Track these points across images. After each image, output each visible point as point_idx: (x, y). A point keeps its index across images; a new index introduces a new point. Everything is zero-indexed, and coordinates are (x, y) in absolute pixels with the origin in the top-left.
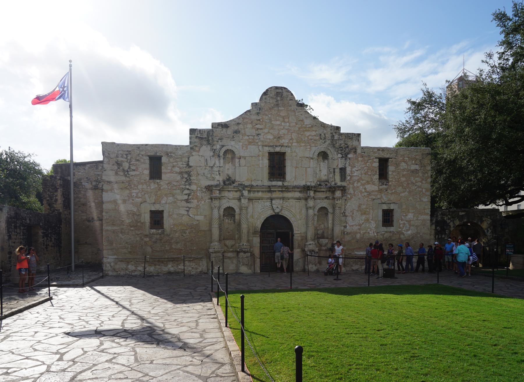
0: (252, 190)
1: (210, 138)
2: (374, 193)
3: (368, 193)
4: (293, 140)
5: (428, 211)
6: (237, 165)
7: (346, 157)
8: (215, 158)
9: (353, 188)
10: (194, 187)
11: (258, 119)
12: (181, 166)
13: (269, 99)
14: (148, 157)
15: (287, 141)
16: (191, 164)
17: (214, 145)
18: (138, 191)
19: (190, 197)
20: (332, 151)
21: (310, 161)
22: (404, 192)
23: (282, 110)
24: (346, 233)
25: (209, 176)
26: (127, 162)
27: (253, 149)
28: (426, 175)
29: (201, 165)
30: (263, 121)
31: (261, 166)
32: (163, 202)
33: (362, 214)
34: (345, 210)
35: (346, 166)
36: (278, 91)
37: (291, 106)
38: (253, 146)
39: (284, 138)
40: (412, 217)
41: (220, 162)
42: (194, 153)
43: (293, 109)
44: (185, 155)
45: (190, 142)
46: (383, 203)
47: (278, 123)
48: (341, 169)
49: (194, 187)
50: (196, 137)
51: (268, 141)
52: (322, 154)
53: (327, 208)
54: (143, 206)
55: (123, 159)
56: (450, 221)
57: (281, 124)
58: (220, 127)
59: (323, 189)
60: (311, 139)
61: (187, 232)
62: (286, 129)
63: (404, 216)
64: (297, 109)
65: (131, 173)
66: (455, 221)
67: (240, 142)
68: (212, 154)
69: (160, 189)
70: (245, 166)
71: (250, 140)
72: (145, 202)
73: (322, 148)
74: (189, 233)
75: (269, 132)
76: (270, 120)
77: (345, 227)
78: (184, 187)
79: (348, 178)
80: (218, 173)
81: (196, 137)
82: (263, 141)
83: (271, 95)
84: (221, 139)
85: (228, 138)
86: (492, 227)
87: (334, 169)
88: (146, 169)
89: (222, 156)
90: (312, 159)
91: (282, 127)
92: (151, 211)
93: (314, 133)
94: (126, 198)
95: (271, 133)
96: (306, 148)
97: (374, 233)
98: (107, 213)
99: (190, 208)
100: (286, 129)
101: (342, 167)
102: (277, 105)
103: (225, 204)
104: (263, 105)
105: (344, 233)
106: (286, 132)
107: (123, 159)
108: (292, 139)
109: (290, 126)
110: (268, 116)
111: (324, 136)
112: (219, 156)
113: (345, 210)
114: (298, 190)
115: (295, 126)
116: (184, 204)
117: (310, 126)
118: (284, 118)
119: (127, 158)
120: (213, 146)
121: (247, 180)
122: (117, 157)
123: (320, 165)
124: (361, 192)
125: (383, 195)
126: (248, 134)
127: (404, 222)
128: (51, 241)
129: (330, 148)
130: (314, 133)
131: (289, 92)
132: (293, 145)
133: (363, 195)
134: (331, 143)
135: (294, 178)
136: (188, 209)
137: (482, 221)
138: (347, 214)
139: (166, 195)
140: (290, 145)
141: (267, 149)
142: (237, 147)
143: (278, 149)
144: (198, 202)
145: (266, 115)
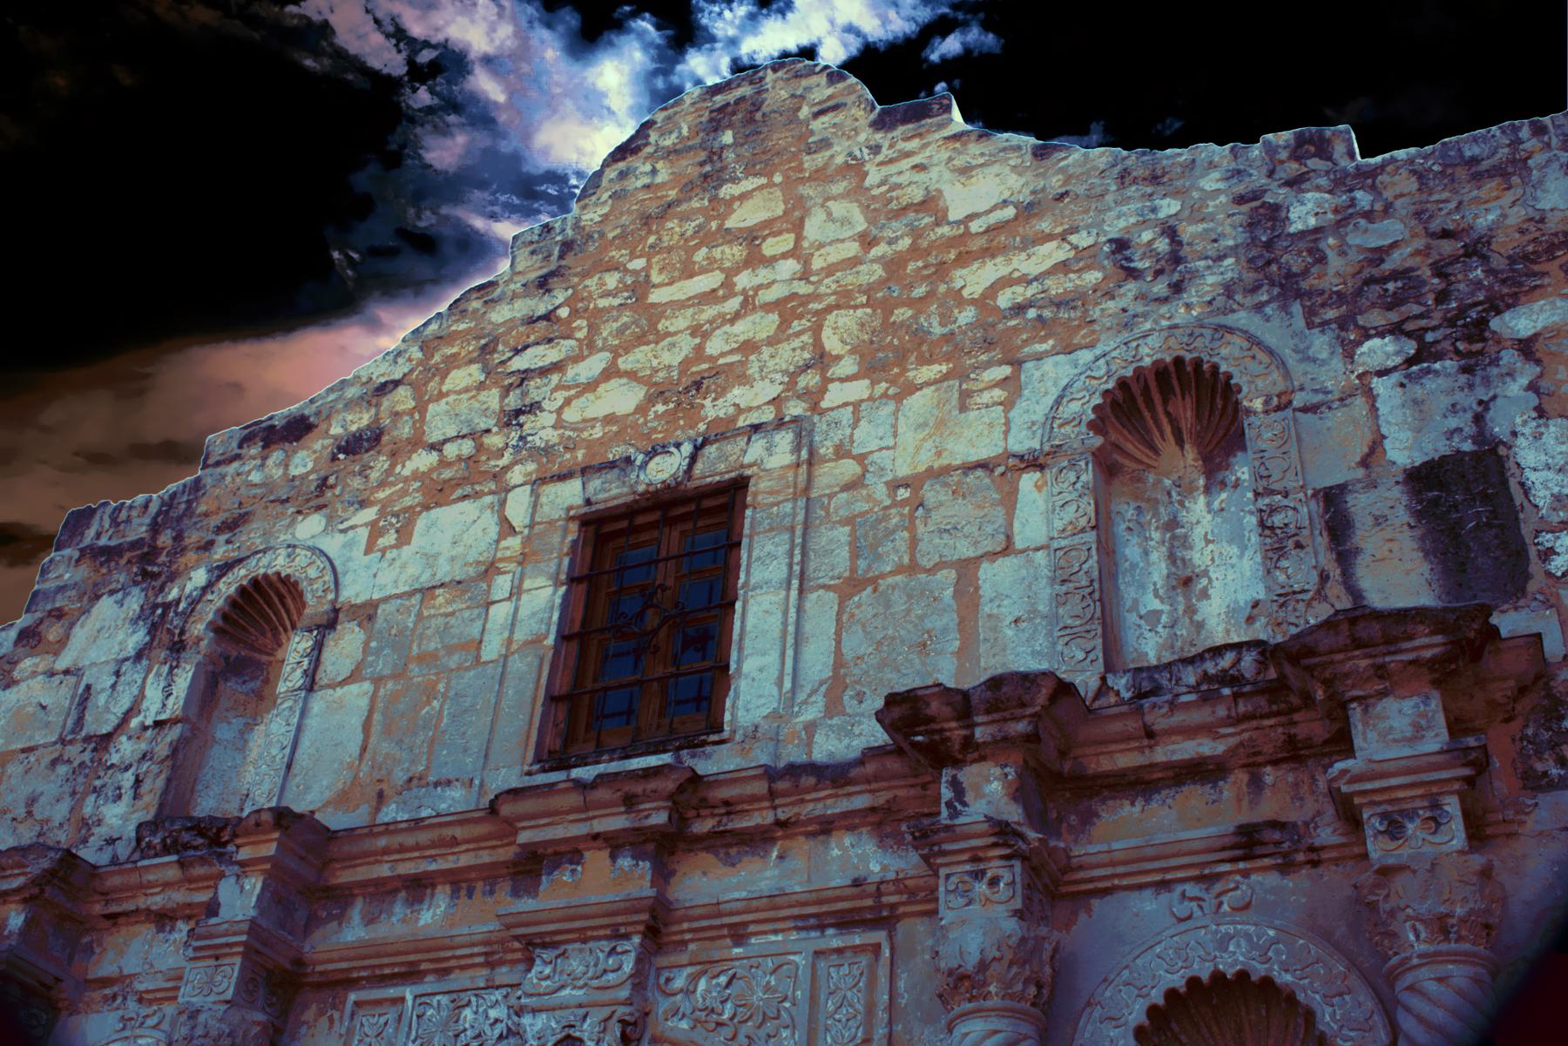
0: (345, 877)
4: (824, 371)
7: (1470, 339)
8: (149, 671)
15: (775, 390)
20: (1271, 340)
21: (1010, 500)
23: (744, 197)
30: (575, 313)
31: (491, 650)
35: (1499, 429)
38: (466, 505)
39: (744, 380)
43: (840, 160)
51: (598, 432)
53: (1291, 999)
57: (728, 285)
59: (1190, 732)
60: (1019, 309)
62: (768, 307)
64: (875, 150)
70: (354, 677)
71: (447, 474)
75: (609, 373)
76: (640, 287)
82: (548, 450)
85: (287, 500)
89: (199, 639)
91: (733, 304)
95: (632, 375)
96: (965, 396)
100: (768, 307)
101: (1434, 446)
102: (706, 177)
109: (804, 276)
110: (626, 270)
111: (1163, 245)
114: (843, 805)
115: (854, 262)
117: (1010, 212)
120: (162, 589)
123: (1173, 524)
126: (434, 436)
129: (1241, 318)
132: (824, 404)
134: (1250, 277)
135: (819, 701)
140: (795, 409)
142: (333, 545)
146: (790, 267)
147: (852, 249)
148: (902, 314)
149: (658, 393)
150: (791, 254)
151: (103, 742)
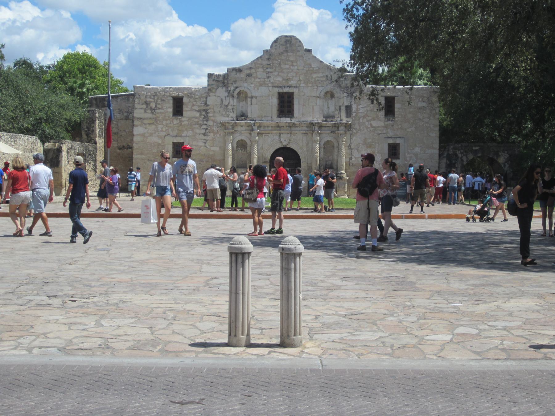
1: (226, 81)
2: (380, 129)
3: (374, 129)
5: (437, 146)
6: (249, 103)
9: (359, 123)
10: (210, 123)
11: (269, 63)
12: (200, 105)
13: (278, 46)
14: (172, 98)
16: (208, 103)
17: (228, 87)
18: (162, 126)
19: (207, 131)
21: (317, 100)
22: (410, 128)
24: (351, 164)
25: (224, 113)
26: (154, 102)
27: (264, 90)
28: (434, 112)
29: (217, 104)
31: (270, 104)
32: (184, 135)
33: (367, 147)
34: (351, 143)
35: (352, 104)
36: (287, 38)
37: (299, 51)
40: (419, 150)
41: (233, 101)
42: (211, 94)
44: (203, 96)
45: (208, 85)
46: (389, 138)
47: (287, 66)
48: (346, 107)
49: (210, 123)
50: (213, 80)
51: (278, 82)
52: (330, 92)
54: (167, 138)
55: (151, 100)
56: (462, 155)
58: (234, 72)
60: (318, 80)
61: (204, 161)
63: (410, 150)
65: (158, 111)
66: (468, 156)
67: (252, 83)
68: (226, 94)
69: (181, 125)
71: (261, 83)
72: (169, 135)
73: (329, 87)
74: (206, 161)
75: (278, 75)
76: (280, 64)
77: (351, 159)
78: (202, 122)
79: (354, 114)
80: (232, 111)
81: (213, 80)
82: (272, 83)
83: (281, 43)
84: (235, 82)
86: (509, 162)
87: (340, 107)
88: (170, 108)
90: (319, 97)
91: (291, 70)
92: (173, 143)
93: (320, 75)
94: (153, 132)
97: (379, 164)
98: (136, 144)
99: (207, 140)
103: (238, 137)
104: (273, 51)
105: (350, 164)
106: (294, 74)
107: (151, 100)
108: (300, 80)
109: (298, 69)
112: (233, 96)
113: (351, 143)
115: (303, 69)
116: (202, 137)
117: (317, 68)
118: (292, 62)
119: (154, 99)
121: (258, 117)
122: (146, 97)
124: (367, 128)
125: (389, 130)
126: (259, 77)
127: (411, 155)
128: (90, 166)
130: (320, 75)
131: (296, 39)
133: (369, 130)
136: (205, 141)
137: (498, 156)
138: (351, 147)
139: (186, 130)
140: (298, 85)
141: (276, 90)
142: (249, 88)
143: (286, 90)
144: (214, 135)
145: (277, 60)
146: (296, 67)
147: (302, 68)
148: (308, 77)
149: (284, 79)
150: (297, 65)
151: (227, 106)
